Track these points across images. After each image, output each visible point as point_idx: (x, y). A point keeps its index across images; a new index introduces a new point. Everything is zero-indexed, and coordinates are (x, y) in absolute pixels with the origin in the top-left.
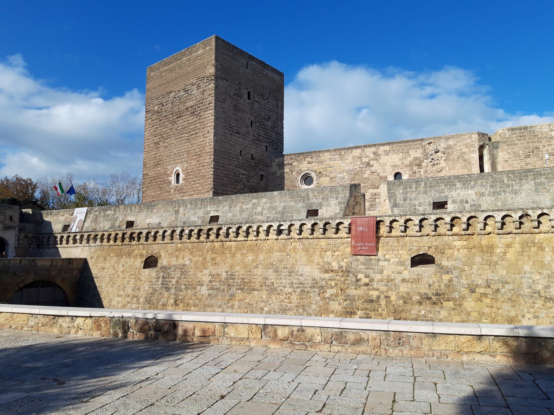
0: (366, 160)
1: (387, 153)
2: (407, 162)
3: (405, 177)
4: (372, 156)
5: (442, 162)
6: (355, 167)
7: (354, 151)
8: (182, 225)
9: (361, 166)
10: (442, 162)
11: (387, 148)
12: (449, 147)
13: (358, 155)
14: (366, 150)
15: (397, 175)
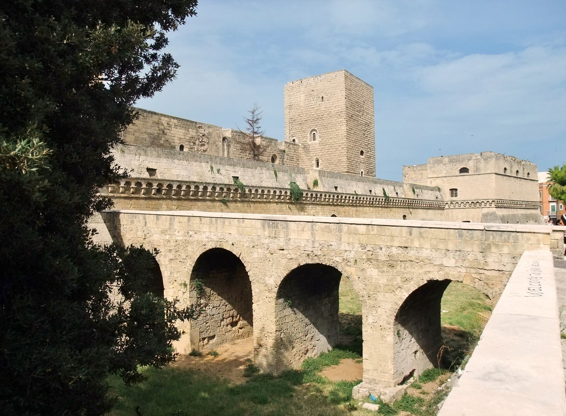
0: (162, 127)
1: (176, 126)
2: (187, 138)
3: (185, 150)
4: (166, 125)
5: (206, 144)
6: (155, 132)
7: (154, 116)
8: (212, 182)
9: (159, 132)
10: (206, 144)
11: (175, 121)
12: (209, 134)
13: (156, 120)
14: (162, 118)
15: (182, 147)
